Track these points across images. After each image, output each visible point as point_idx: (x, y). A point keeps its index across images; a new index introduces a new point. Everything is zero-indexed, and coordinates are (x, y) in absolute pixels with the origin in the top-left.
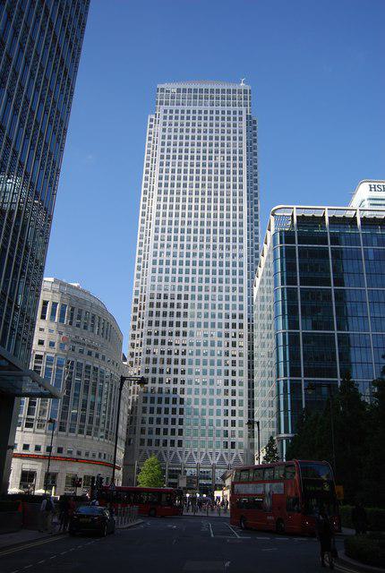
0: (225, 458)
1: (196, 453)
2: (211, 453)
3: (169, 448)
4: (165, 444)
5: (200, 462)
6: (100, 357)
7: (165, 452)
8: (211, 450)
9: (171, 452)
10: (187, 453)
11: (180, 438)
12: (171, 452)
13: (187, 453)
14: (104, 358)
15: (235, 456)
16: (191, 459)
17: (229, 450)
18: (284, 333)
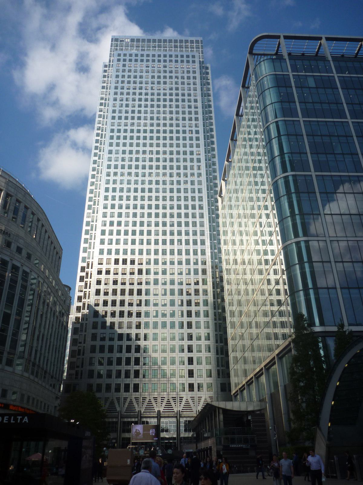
1: (155, 399)
2: (174, 398)
3: (123, 394)
4: (118, 390)
5: (162, 410)
6: (14, 247)
7: (118, 399)
8: (174, 394)
9: (125, 399)
10: (144, 399)
11: (136, 381)
12: (125, 399)
13: (144, 399)
14: (19, 250)
16: (150, 406)
17: (196, 393)
18: (286, 178)
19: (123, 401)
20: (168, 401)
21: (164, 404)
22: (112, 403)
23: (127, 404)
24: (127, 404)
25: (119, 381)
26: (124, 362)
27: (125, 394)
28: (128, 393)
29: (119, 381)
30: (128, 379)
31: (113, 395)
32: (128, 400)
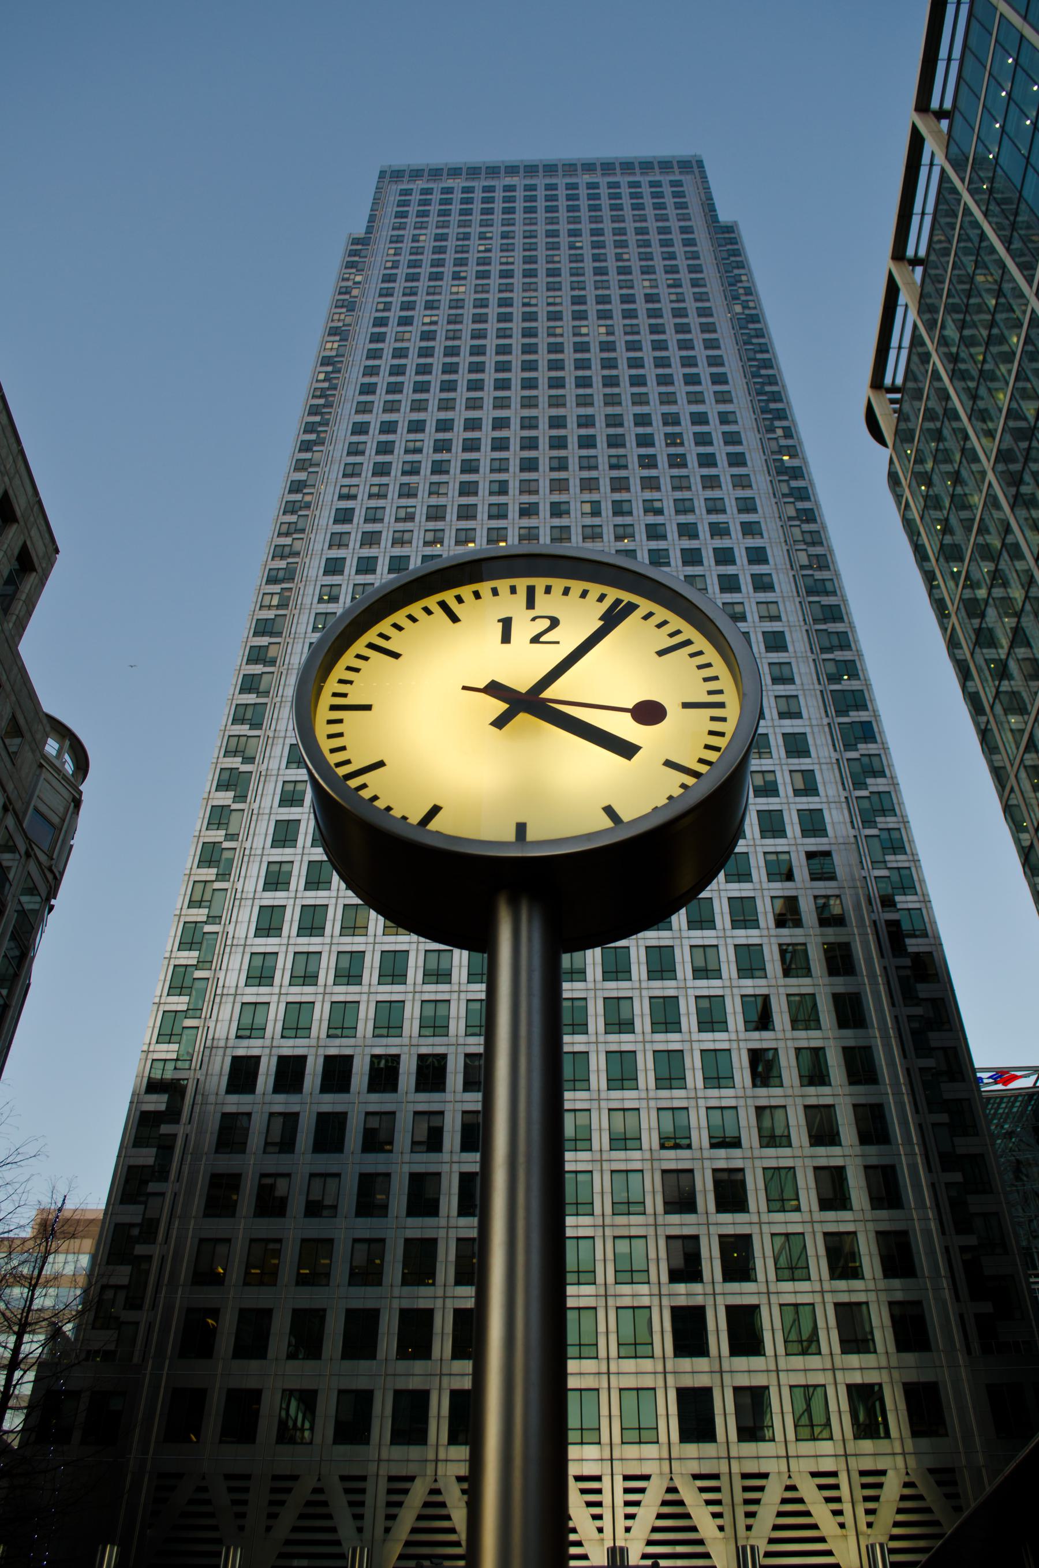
0: (821, 1513)
3: (383, 1454)
4: (353, 1425)
7: (355, 1486)
15: (892, 1489)
19: (382, 1497)
20: (673, 1505)
21: (647, 1514)
22: (317, 1508)
23: (407, 1519)
24: (407, 1519)
25: (360, 1374)
26: (394, 1269)
27: (399, 1452)
28: (414, 1452)
29: (360, 1374)
30: (419, 1366)
31: (321, 1453)
32: (418, 1493)
